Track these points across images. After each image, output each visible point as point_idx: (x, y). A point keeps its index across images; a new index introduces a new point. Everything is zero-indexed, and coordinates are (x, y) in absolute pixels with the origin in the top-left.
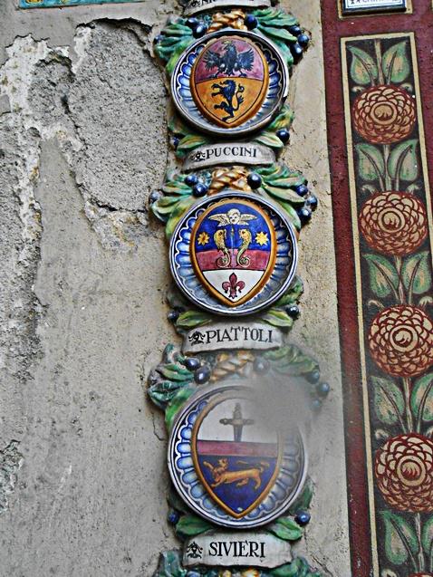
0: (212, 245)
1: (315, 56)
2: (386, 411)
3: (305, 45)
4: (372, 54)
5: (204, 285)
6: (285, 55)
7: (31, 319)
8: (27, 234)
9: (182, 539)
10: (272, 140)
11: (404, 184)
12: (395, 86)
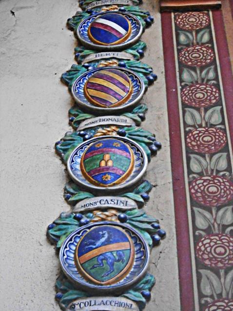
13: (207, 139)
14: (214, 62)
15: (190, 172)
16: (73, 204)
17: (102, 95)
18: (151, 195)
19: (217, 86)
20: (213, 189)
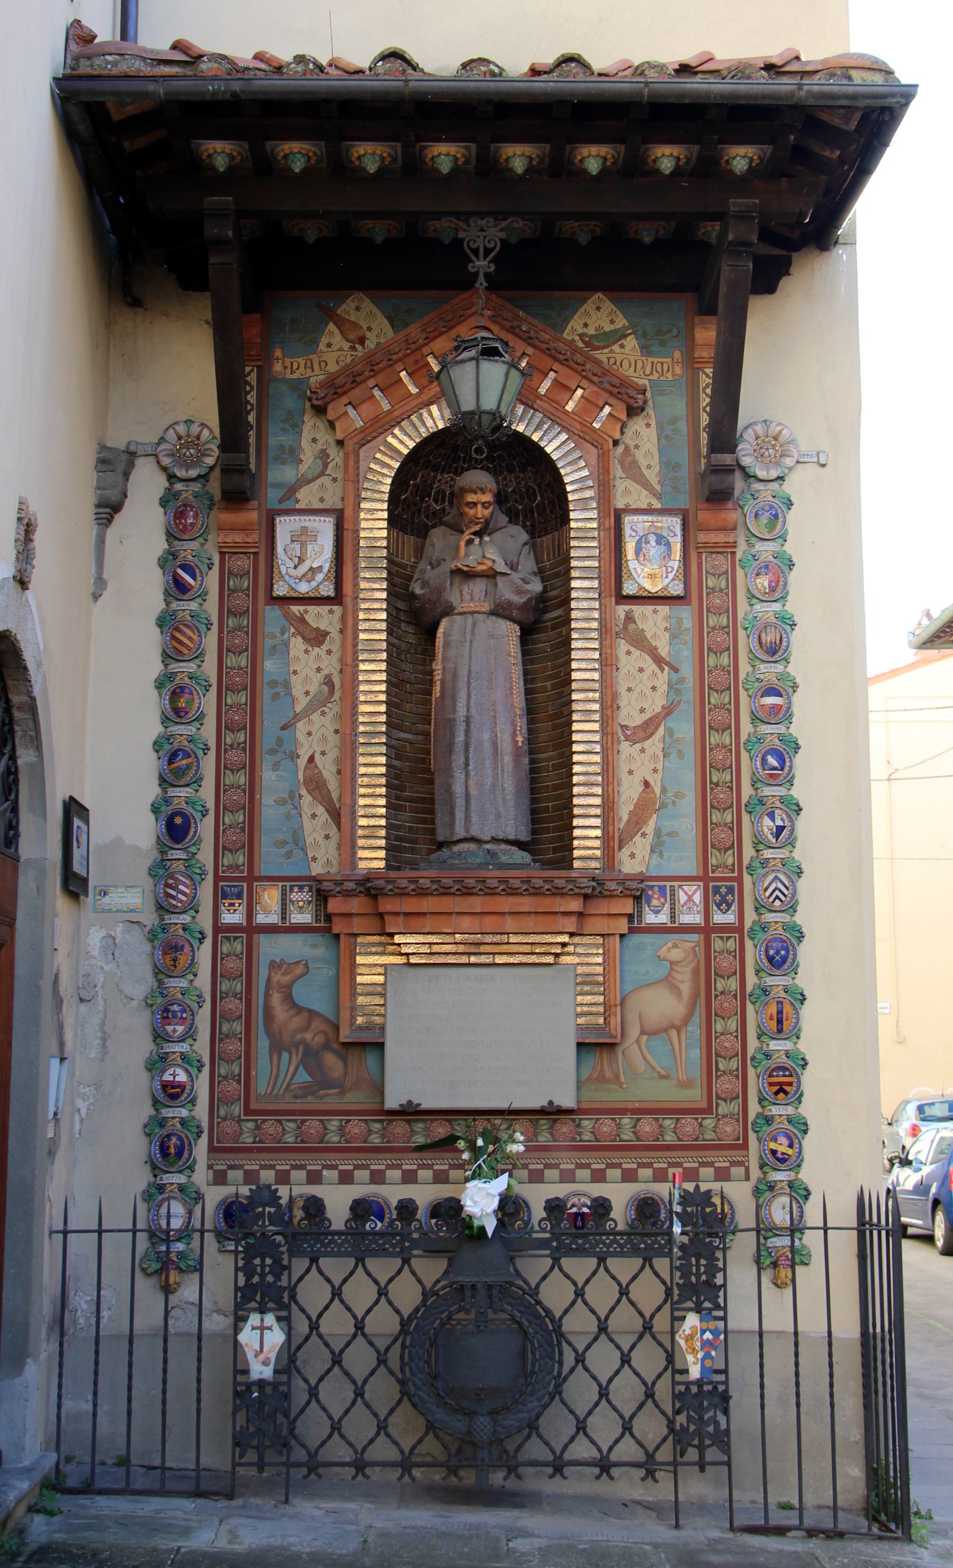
0: (167, 1017)
1: (208, 942)
2: (223, 1072)
3: (204, 938)
4: (230, 941)
5: (165, 1029)
6: (196, 943)
7: (104, 1039)
8: (101, 1008)
9: (157, 1110)
10: (191, 977)
11: (236, 994)
12: (237, 956)
13: (237, 679)
14: (248, 610)
15: (226, 705)
16: (166, 727)
17: (179, 647)
18: (205, 721)
19: (247, 633)
20: (236, 718)
